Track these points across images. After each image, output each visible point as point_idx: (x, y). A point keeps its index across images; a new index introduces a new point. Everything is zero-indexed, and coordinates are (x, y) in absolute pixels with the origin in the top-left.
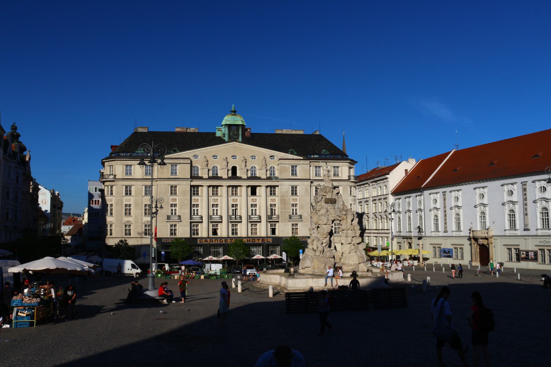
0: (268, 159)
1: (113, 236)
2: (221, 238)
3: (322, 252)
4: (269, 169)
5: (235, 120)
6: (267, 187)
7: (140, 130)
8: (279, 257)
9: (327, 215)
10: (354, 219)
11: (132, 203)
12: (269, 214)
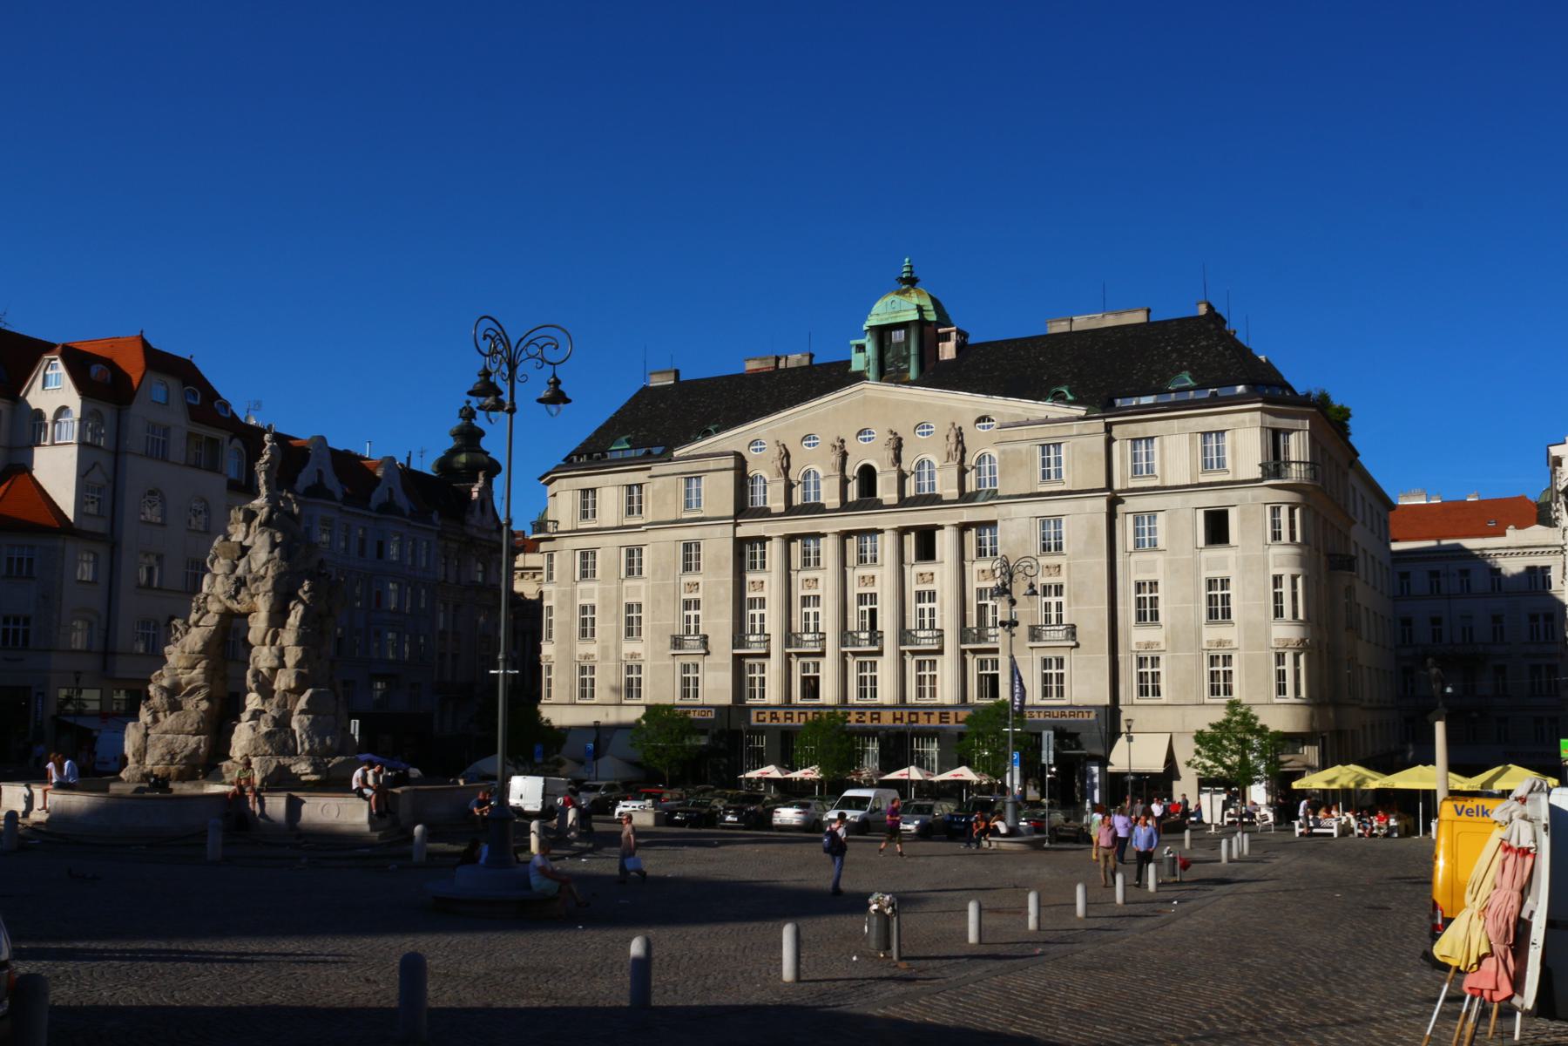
4: (974, 464)
5: (896, 310)
7: (657, 381)
12: (972, 621)
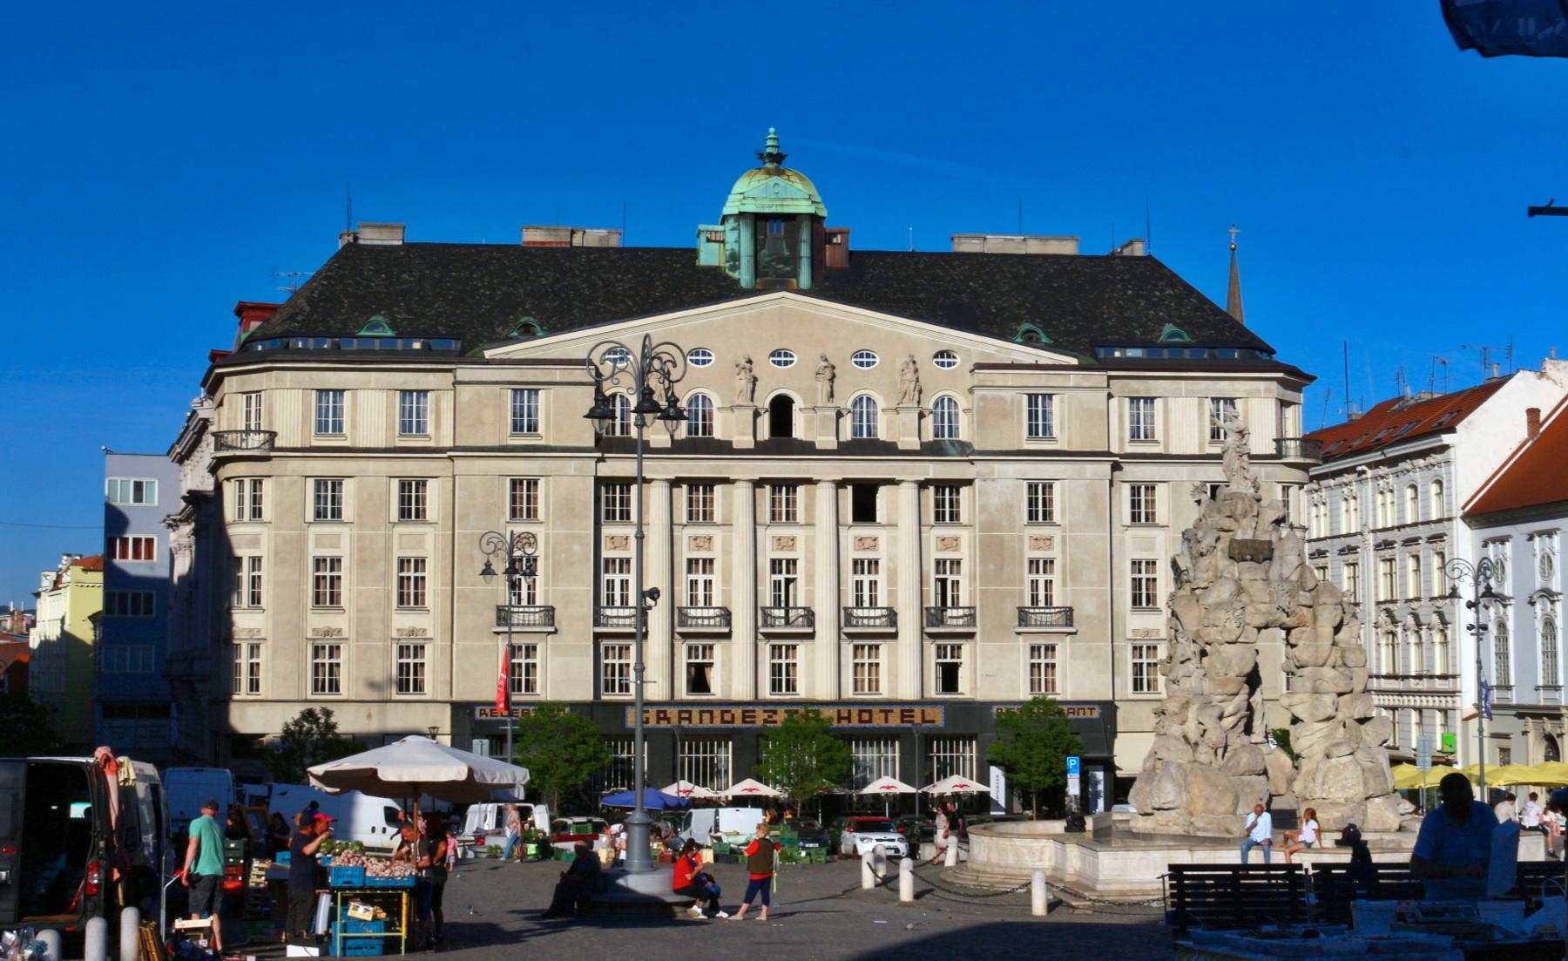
0: (928, 366)
1: (264, 692)
2: (728, 704)
3: (1220, 752)
5: (780, 196)
6: (923, 485)
7: (369, 237)
8: (975, 787)
9: (1238, 605)
10: (1345, 622)
11: (344, 551)
12: (932, 601)
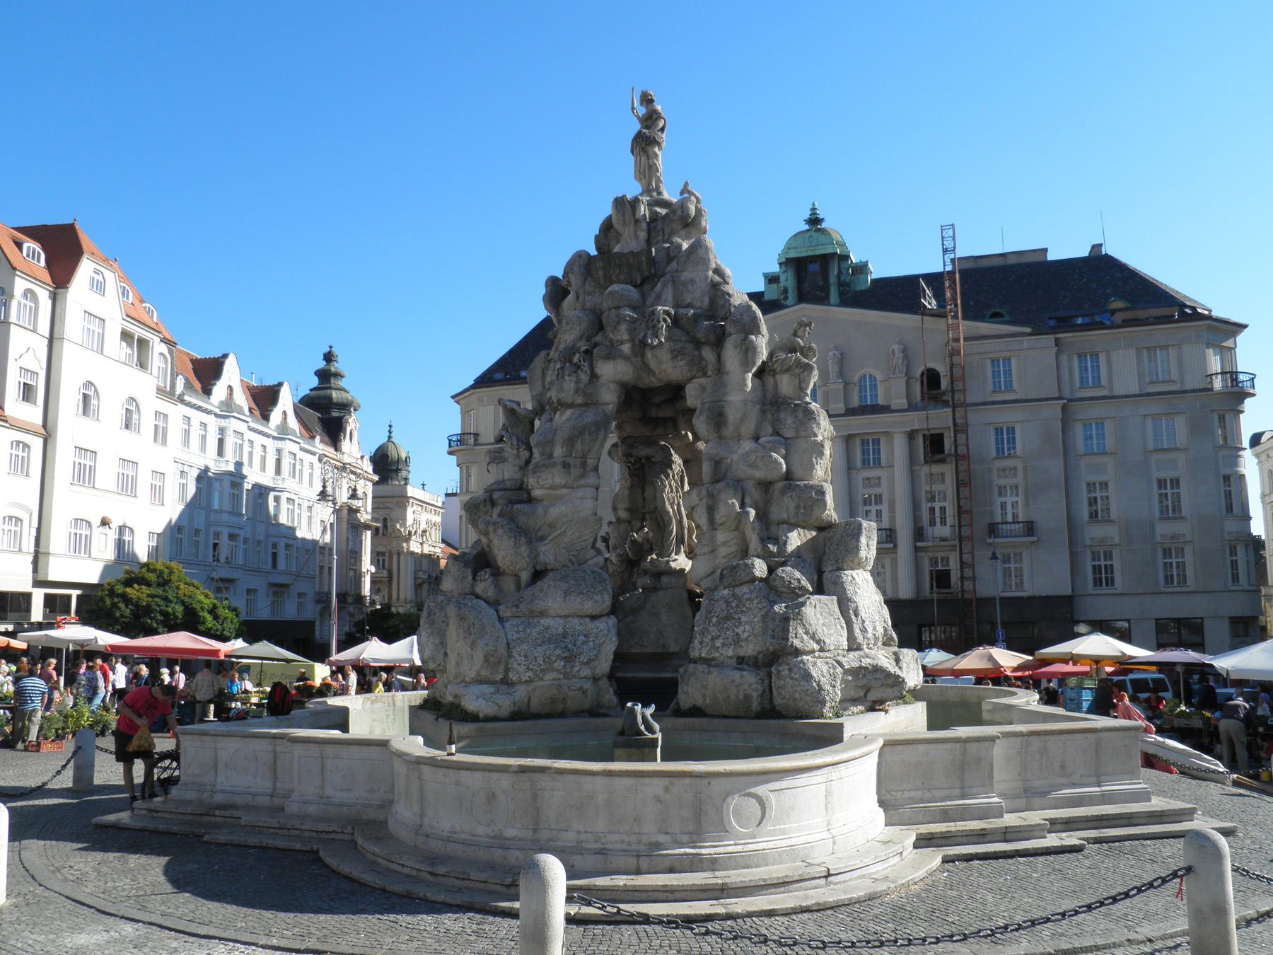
5: (813, 244)
